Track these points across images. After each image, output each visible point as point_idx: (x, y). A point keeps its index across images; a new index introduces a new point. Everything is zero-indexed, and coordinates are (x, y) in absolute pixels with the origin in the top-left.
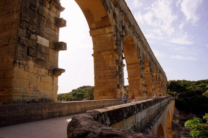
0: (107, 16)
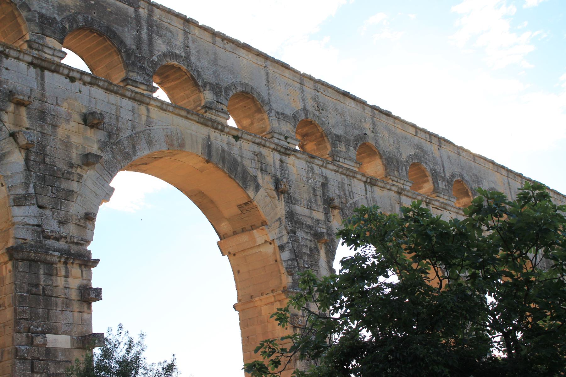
0: (251, 202)
